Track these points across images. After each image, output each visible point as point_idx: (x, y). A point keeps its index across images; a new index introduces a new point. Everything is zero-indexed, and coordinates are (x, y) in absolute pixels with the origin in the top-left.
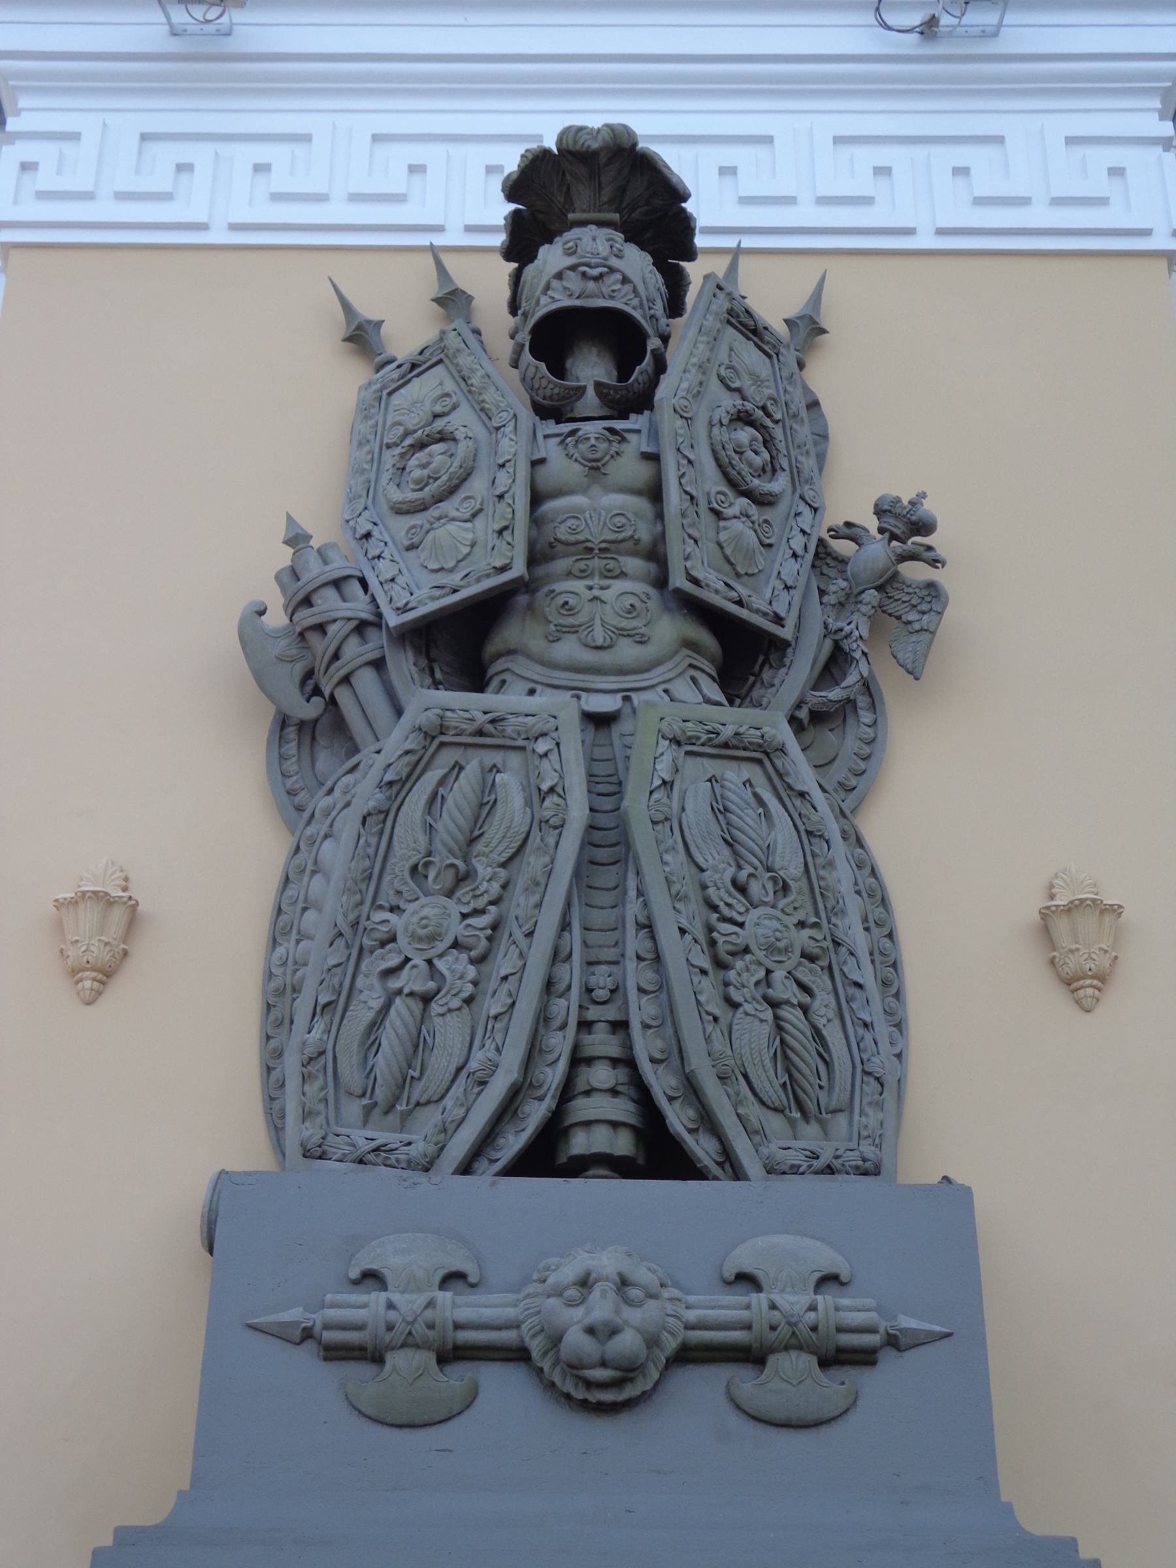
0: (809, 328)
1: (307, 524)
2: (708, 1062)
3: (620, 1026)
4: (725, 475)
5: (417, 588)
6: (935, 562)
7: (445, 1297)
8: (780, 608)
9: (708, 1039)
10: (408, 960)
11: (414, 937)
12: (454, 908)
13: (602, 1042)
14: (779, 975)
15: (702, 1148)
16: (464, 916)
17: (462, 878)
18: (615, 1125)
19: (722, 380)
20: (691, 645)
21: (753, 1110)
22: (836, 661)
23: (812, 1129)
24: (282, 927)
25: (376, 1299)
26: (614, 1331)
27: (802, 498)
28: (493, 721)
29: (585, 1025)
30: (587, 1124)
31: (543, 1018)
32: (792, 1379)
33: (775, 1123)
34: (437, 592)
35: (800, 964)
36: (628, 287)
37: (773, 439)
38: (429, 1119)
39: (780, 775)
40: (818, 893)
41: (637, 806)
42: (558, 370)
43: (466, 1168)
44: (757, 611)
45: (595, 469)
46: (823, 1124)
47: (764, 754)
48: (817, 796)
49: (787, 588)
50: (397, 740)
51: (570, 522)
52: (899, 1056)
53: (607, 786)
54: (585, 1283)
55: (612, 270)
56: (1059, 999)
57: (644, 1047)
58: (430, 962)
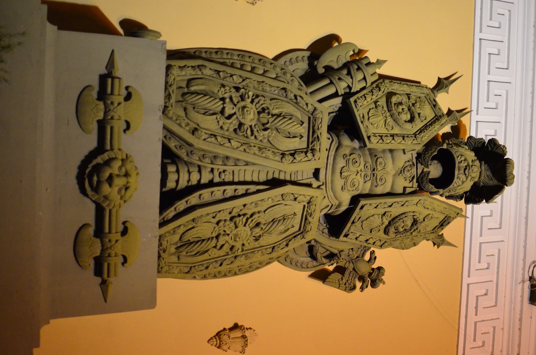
2: (199, 215)
4: (397, 217)
6: (362, 289)
8: (351, 236)
9: (208, 214)
10: (235, 105)
14: (227, 238)
15: (170, 213)
16: (251, 126)
18: (177, 182)
19: (428, 215)
20: (339, 205)
23: (173, 250)
26: (110, 185)
27: (385, 242)
28: (318, 137)
30: (178, 171)
33: (176, 238)
34: (362, 116)
35: (230, 245)
36: (461, 183)
39: (294, 237)
40: (253, 251)
43: (165, 128)
44: (350, 228)
47: (302, 231)
48: (286, 249)
49: (356, 238)
51: (383, 162)
52: (195, 277)
55: (467, 178)
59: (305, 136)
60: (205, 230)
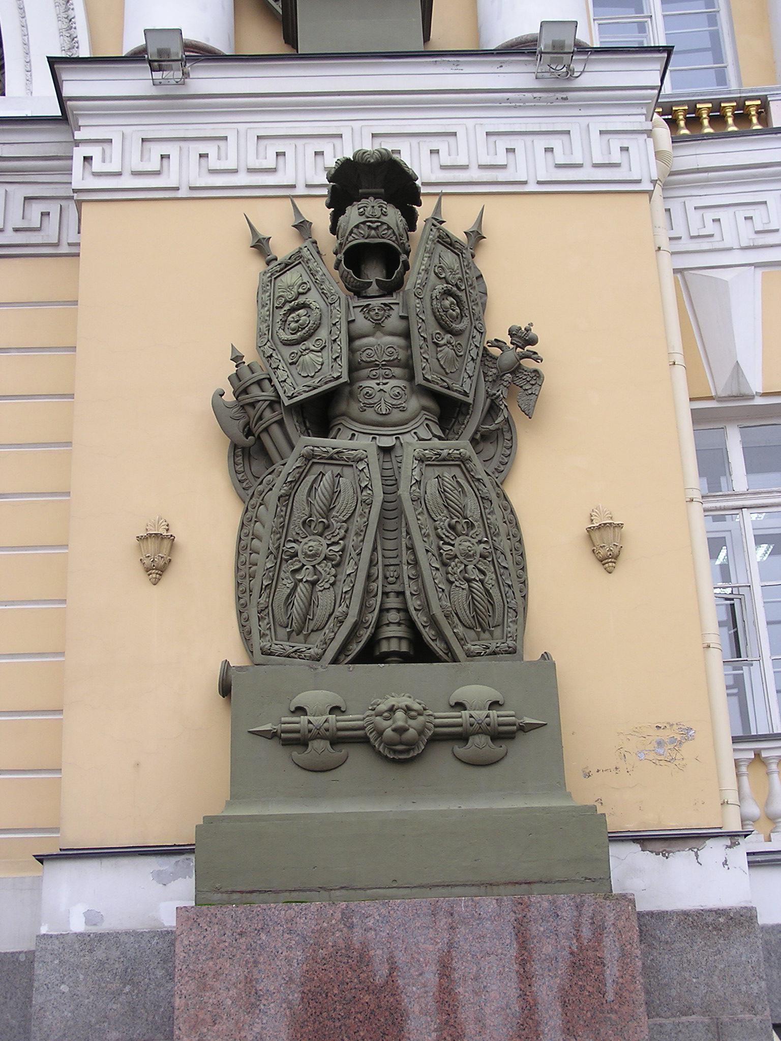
0: (476, 236)
1: (242, 351)
2: (440, 610)
3: (401, 594)
4: (439, 324)
5: (296, 386)
6: (538, 360)
7: (332, 717)
9: (440, 599)
10: (304, 565)
11: (306, 555)
12: (325, 542)
13: (393, 602)
14: (470, 567)
15: (437, 647)
16: (329, 545)
17: (327, 527)
19: (436, 274)
20: (424, 408)
21: (460, 630)
22: (493, 409)
23: (487, 635)
24: (242, 548)
25: (303, 719)
26: (406, 730)
27: (475, 327)
28: (337, 453)
29: (385, 594)
30: (388, 638)
31: (367, 591)
32: (480, 744)
33: (472, 634)
34: (307, 389)
36: (390, 231)
37: (462, 299)
38: (318, 638)
39: (469, 472)
40: (487, 526)
41: (404, 491)
42: (358, 273)
43: (335, 661)
44: (456, 391)
45: (378, 325)
46: (491, 633)
47: (462, 462)
48: (486, 479)
49: (470, 377)
50: (293, 462)
51: (368, 351)
52: (524, 597)
53: (391, 483)
54: (392, 710)
55: (383, 223)
56: (597, 570)
57: (413, 603)
58: (314, 566)
59: (337, 470)
60: (460, 596)
